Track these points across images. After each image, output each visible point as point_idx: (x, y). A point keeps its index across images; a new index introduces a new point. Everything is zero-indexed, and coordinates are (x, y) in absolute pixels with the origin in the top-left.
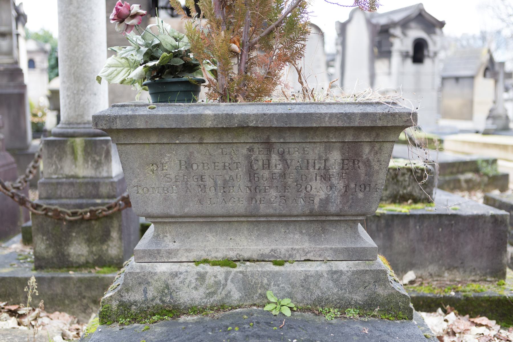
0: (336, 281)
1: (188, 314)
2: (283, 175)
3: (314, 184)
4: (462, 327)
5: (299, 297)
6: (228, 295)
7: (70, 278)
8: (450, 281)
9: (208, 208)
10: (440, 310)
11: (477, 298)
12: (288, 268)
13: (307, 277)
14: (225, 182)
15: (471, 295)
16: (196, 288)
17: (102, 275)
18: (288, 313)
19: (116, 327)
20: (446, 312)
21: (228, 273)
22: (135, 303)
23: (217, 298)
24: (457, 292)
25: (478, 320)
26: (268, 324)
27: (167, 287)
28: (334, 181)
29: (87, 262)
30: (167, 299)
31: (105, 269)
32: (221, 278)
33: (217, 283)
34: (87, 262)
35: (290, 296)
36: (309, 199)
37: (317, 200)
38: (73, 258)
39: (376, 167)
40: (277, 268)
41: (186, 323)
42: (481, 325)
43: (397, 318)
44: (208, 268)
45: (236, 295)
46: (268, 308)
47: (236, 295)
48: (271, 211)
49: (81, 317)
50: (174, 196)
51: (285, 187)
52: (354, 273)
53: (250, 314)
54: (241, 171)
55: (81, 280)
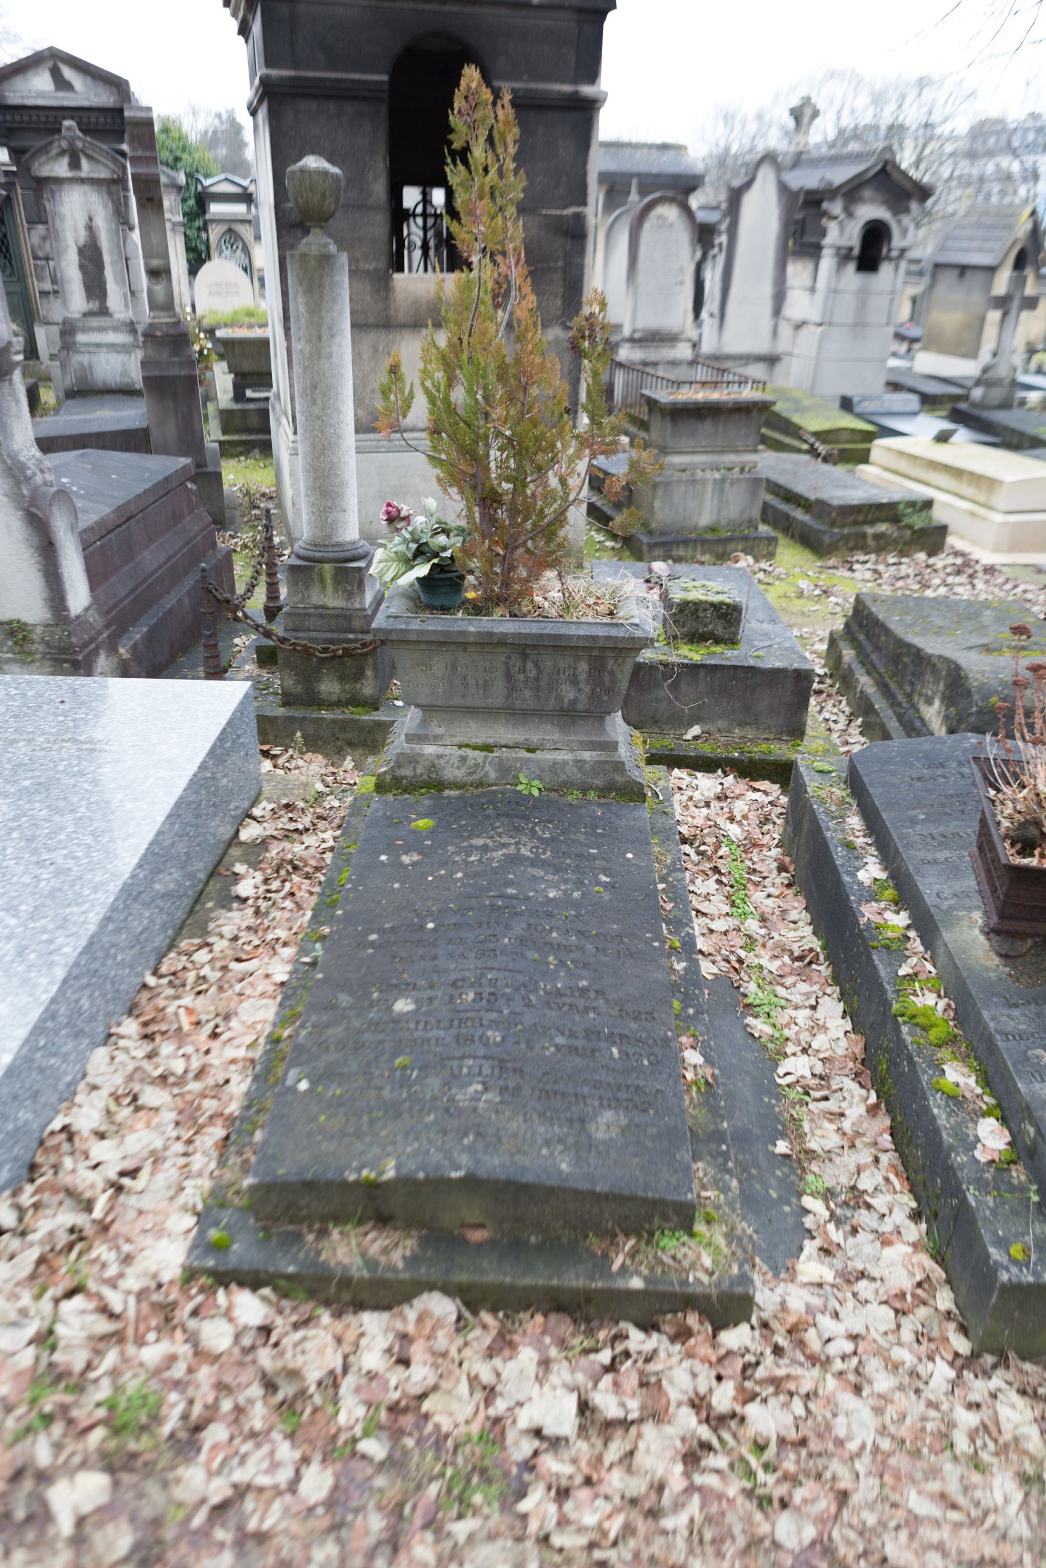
0: (580, 769)
1: (451, 789)
2: (537, 679)
3: (564, 687)
4: (738, 792)
5: (547, 779)
6: (486, 775)
7: (323, 719)
8: (741, 738)
9: (470, 702)
10: (719, 772)
11: (762, 761)
12: (539, 755)
13: (555, 764)
14: (486, 682)
15: (756, 756)
16: (458, 768)
17: (357, 717)
18: (536, 793)
19: (390, 797)
20: (726, 774)
21: (486, 757)
22: (406, 777)
23: (476, 777)
24: (742, 753)
25: (757, 785)
26: (517, 803)
27: (434, 766)
28: (582, 686)
29: (340, 701)
30: (434, 776)
31: (359, 710)
32: (480, 760)
33: (477, 765)
34: (340, 701)
35: (539, 778)
36: (559, 698)
37: (566, 701)
38: (324, 696)
39: (619, 676)
40: (529, 755)
41: (449, 797)
42: (759, 790)
43: (631, 801)
44: (469, 752)
45: (493, 776)
46: (520, 788)
47: (493, 776)
48: (525, 707)
49: (335, 759)
50: (441, 691)
51: (538, 689)
52: (596, 762)
53: (503, 793)
54: (500, 674)
55: (334, 721)
